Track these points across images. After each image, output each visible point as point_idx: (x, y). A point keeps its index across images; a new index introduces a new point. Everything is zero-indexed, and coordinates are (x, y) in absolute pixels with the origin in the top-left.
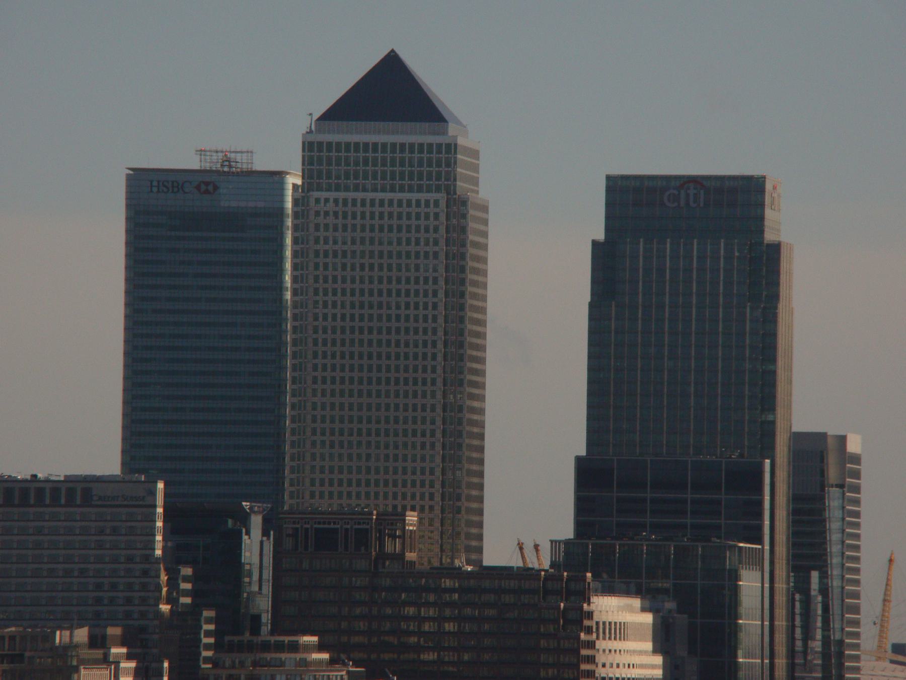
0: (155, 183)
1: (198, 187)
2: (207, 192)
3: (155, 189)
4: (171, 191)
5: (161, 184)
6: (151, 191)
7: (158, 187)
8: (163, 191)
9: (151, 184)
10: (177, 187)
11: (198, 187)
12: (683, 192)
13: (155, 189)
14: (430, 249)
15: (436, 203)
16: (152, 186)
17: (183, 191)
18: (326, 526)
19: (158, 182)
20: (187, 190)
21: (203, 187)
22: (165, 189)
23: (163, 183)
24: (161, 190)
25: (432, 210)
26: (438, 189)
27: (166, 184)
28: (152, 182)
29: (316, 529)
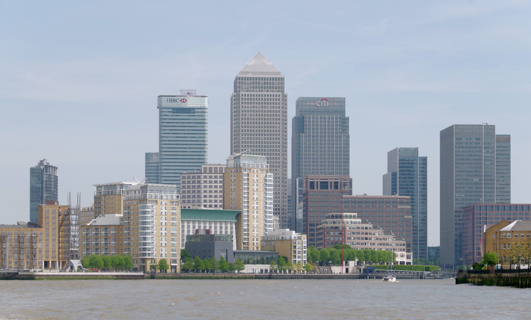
1: (181, 101)
3: (168, 101)
11: (181, 101)
12: (322, 102)
13: (168, 101)
14: (278, 109)
15: (279, 96)
16: (167, 100)
18: (324, 181)
19: (169, 99)
21: (182, 101)
25: (278, 98)
26: (279, 91)
29: (320, 182)
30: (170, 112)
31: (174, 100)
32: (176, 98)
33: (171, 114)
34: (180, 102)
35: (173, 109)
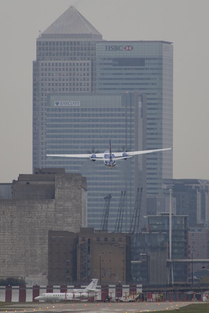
0: (108, 47)
2: (129, 50)
3: (108, 49)
4: (114, 50)
5: (110, 47)
9: (106, 47)
10: (117, 48)
13: (108, 49)
16: (106, 48)
19: (109, 46)
20: (120, 49)
22: (112, 49)
24: (110, 50)
30: (111, 64)
32: (118, 45)
33: (111, 67)
34: (124, 50)
35: (114, 59)
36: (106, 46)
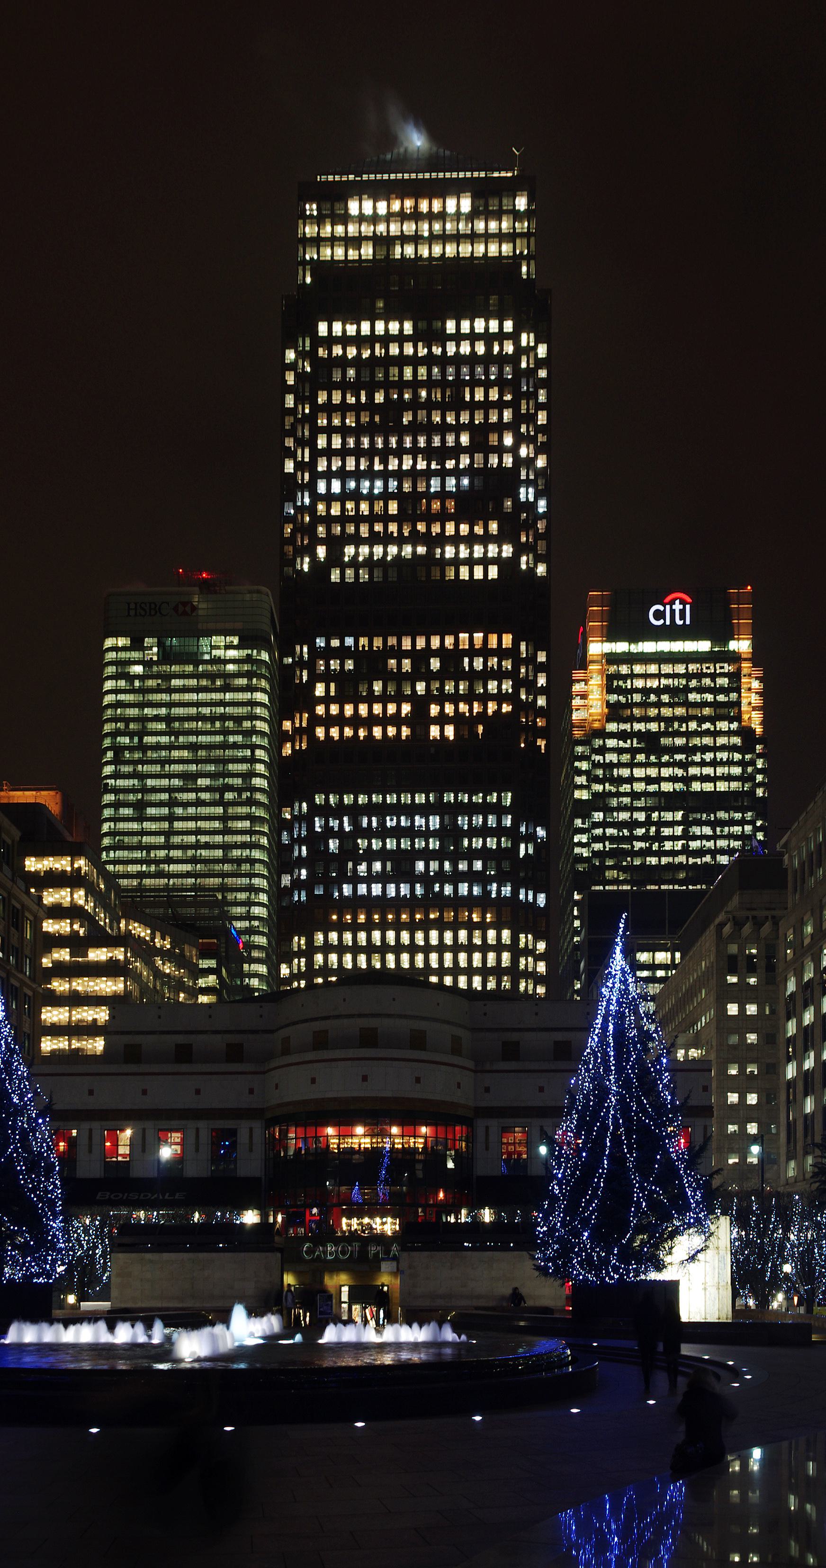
0: (132, 606)
3: (132, 613)
6: (129, 615)
7: (136, 609)
8: (140, 615)
9: (129, 607)
16: (129, 609)
17: (161, 613)
19: (136, 604)
22: (143, 613)
23: (140, 606)
27: (143, 605)
28: (129, 604)
31: (153, 606)
36: (129, 604)
